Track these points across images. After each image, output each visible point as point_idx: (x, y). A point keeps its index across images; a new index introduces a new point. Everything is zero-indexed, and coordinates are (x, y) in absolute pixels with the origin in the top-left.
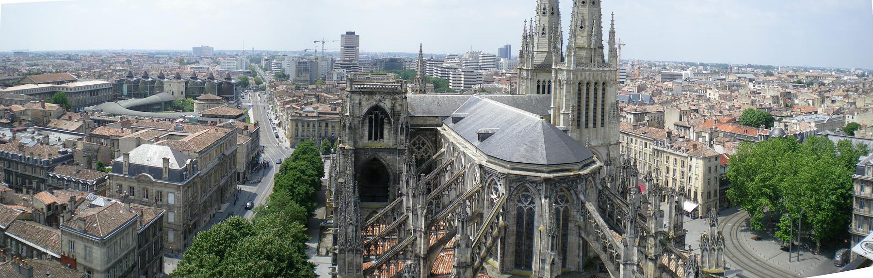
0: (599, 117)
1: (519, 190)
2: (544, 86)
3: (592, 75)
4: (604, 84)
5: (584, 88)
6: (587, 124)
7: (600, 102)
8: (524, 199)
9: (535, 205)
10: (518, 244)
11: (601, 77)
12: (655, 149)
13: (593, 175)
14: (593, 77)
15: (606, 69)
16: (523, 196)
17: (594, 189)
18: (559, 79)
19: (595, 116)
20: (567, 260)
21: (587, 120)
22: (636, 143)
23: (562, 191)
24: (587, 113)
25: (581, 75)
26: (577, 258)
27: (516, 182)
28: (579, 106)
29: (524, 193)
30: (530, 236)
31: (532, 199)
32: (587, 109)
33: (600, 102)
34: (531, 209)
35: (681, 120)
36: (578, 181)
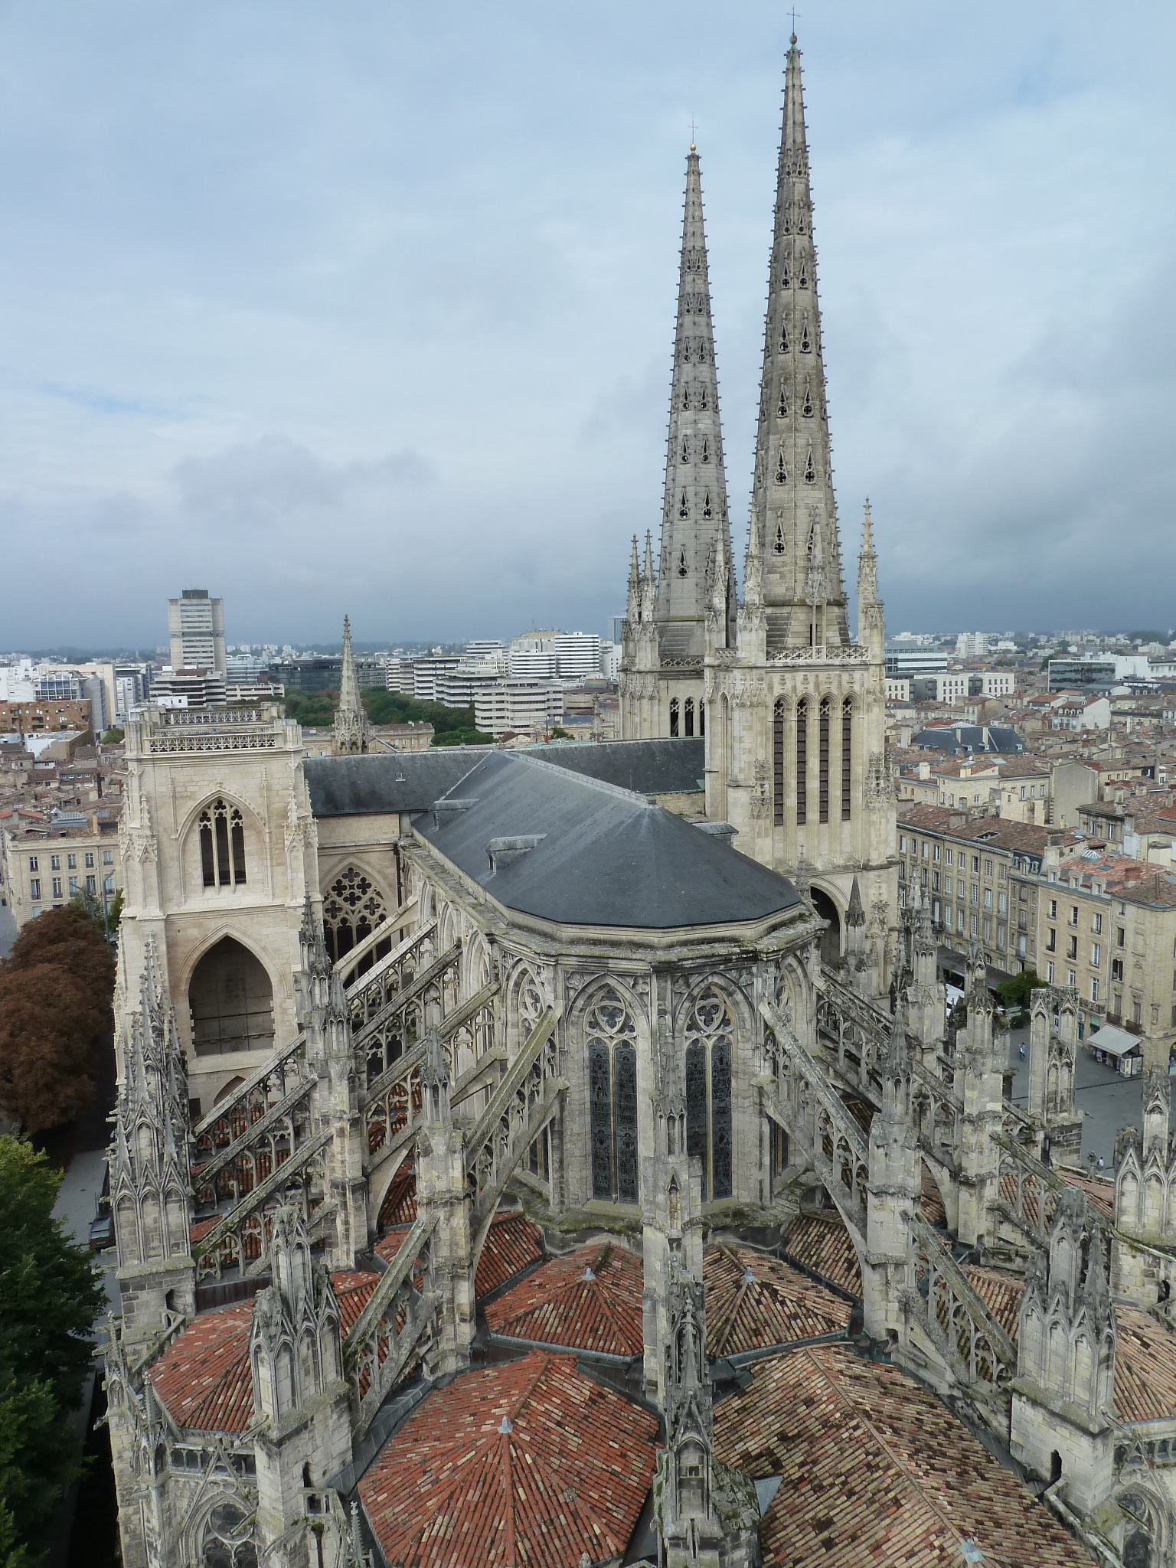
1: (591, 996)
2: (689, 715)
4: (847, 702)
5: (791, 717)
8: (605, 1019)
9: (635, 1034)
10: (599, 1138)
11: (840, 685)
13: (798, 953)
14: (817, 685)
15: (852, 661)
17: (804, 990)
18: (724, 694)
19: (824, 793)
20: (734, 1177)
22: (962, 862)
25: (783, 682)
26: (754, 1170)
27: (582, 974)
28: (779, 763)
29: (606, 1003)
30: (627, 1114)
34: (625, 1043)
36: (754, 970)
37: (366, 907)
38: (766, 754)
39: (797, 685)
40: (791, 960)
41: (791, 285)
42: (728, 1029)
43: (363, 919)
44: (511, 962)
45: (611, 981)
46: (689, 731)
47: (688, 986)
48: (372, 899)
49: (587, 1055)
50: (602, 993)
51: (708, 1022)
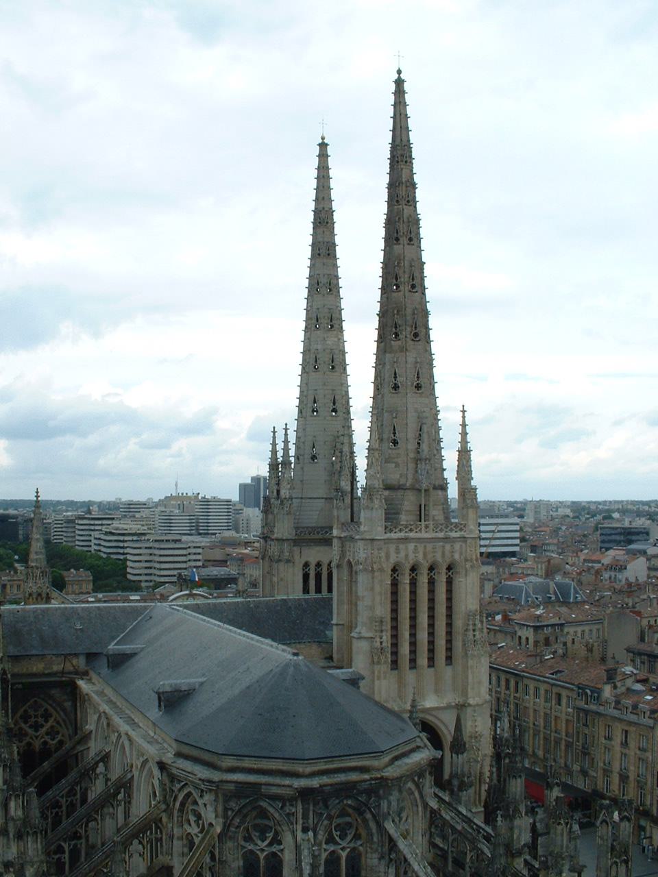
0: (441, 643)
1: (245, 816)
2: (318, 576)
3: (421, 548)
4: (449, 568)
6: (413, 661)
7: (441, 609)
8: (257, 834)
9: (282, 847)
11: (443, 554)
12: (580, 709)
13: (416, 779)
14: (425, 554)
15: (453, 534)
16: (256, 827)
17: (420, 809)
18: (349, 560)
21: (413, 652)
23: (343, 814)
24: (413, 635)
25: (398, 551)
27: (239, 798)
28: (395, 619)
29: (259, 821)
31: (276, 833)
32: (413, 626)
33: (441, 609)
34: (274, 854)
35: (642, 639)
37: (47, 734)
38: (383, 610)
39: (410, 554)
40: (410, 785)
41: (401, 241)
42: (359, 843)
43: (45, 743)
44: (178, 786)
45: (263, 804)
46: (318, 590)
47: (327, 807)
48: (52, 727)
49: (241, 863)
50: (254, 813)
51: (342, 837)
